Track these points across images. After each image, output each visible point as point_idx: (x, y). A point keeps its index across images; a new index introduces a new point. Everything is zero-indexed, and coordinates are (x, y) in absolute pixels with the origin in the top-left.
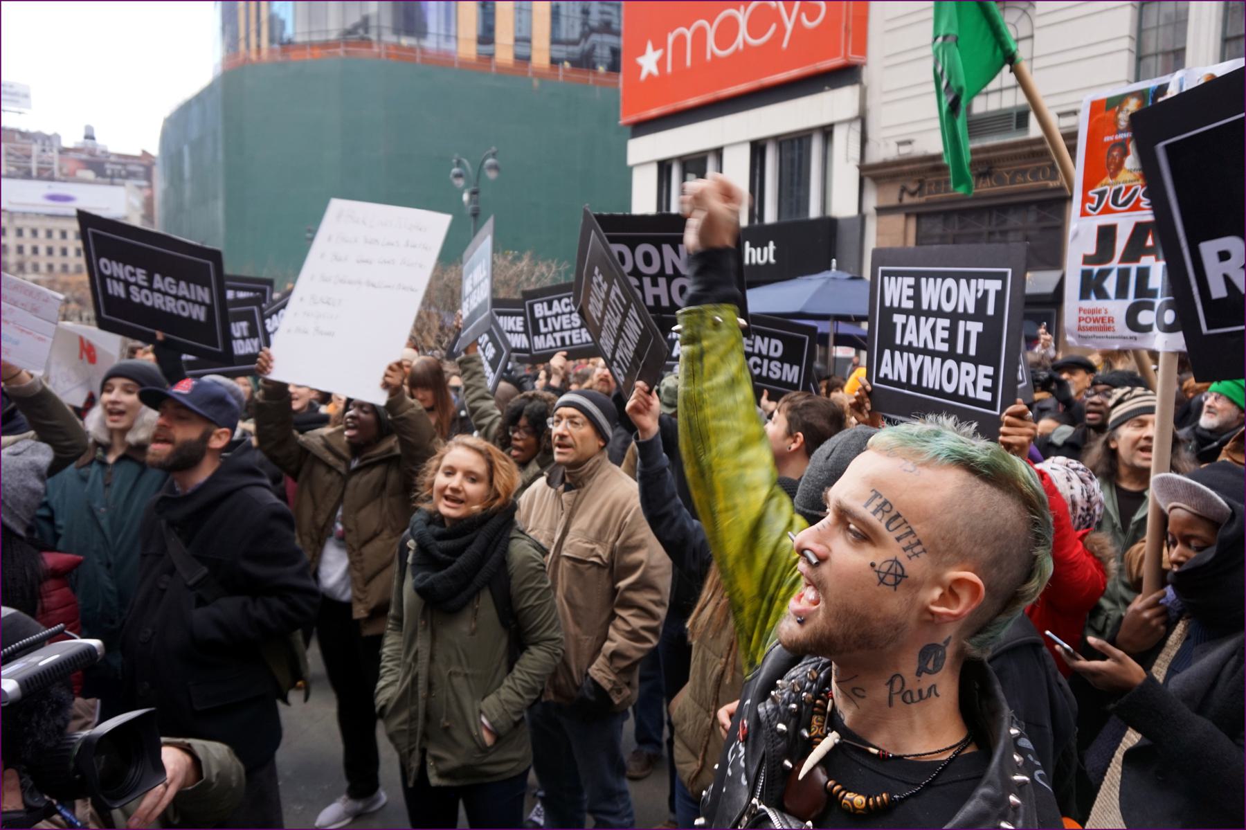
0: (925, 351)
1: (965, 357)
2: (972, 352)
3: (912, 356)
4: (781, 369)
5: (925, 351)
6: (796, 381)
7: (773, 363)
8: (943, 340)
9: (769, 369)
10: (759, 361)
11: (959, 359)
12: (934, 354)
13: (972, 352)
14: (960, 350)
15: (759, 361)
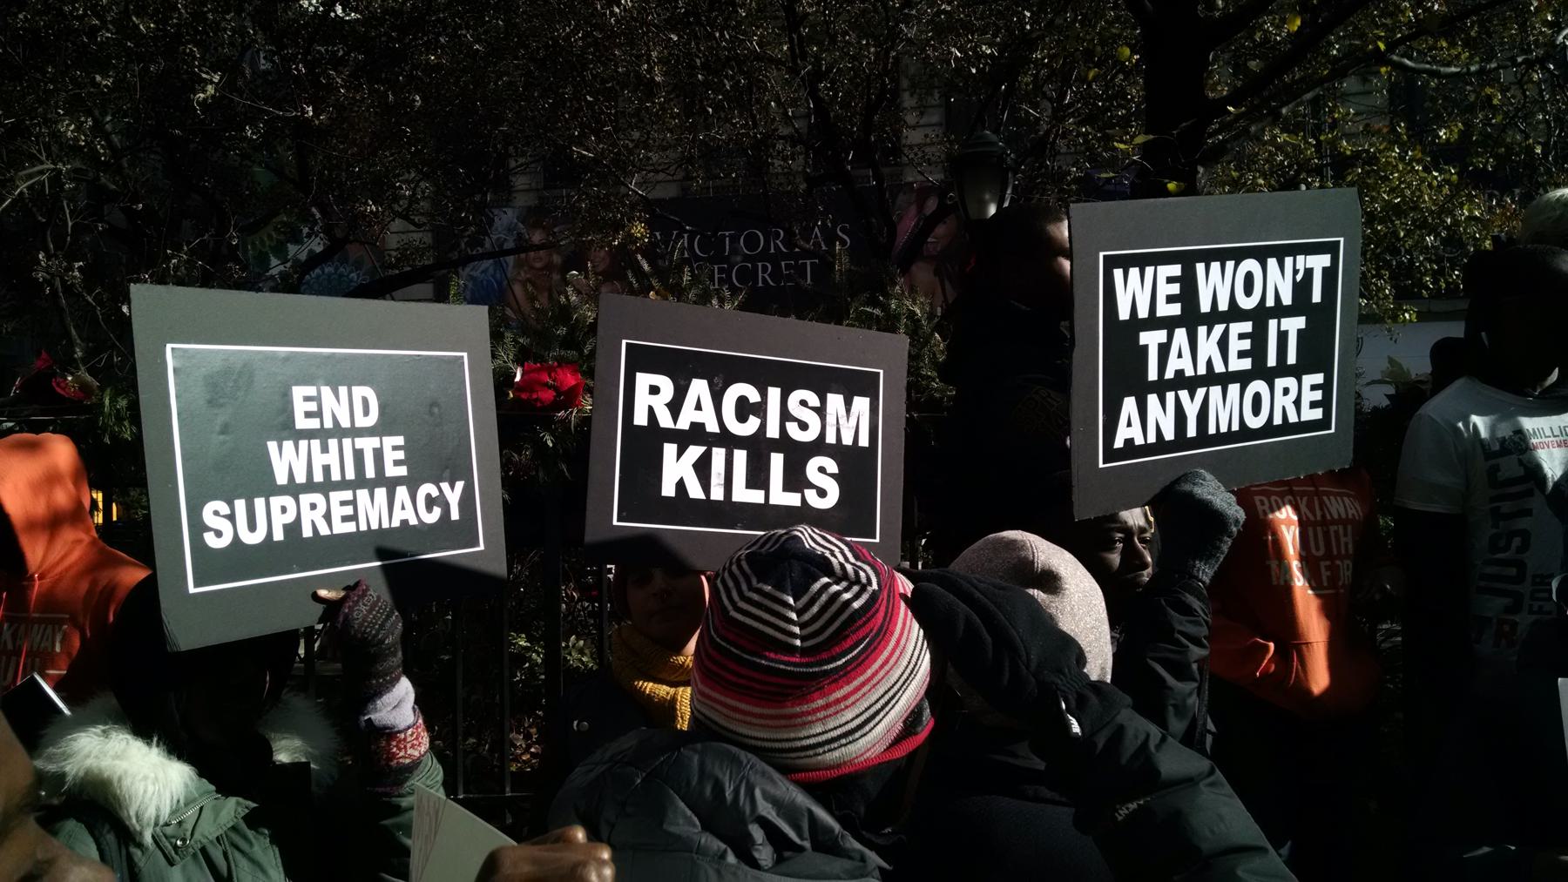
0: (1211, 378)
1: (1283, 369)
2: (1292, 359)
3: (1184, 394)
4: (821, 411)
5: (1211, 378)
6: (864, 442)
7: (797, 396)
8: (1242, 354)
9: (785, 416)
10: (753, 395)
11: (1269, 376)
12: (1225, 380)
13: (1292, 359)
14: (1272, 361)
15: (753, 395)
